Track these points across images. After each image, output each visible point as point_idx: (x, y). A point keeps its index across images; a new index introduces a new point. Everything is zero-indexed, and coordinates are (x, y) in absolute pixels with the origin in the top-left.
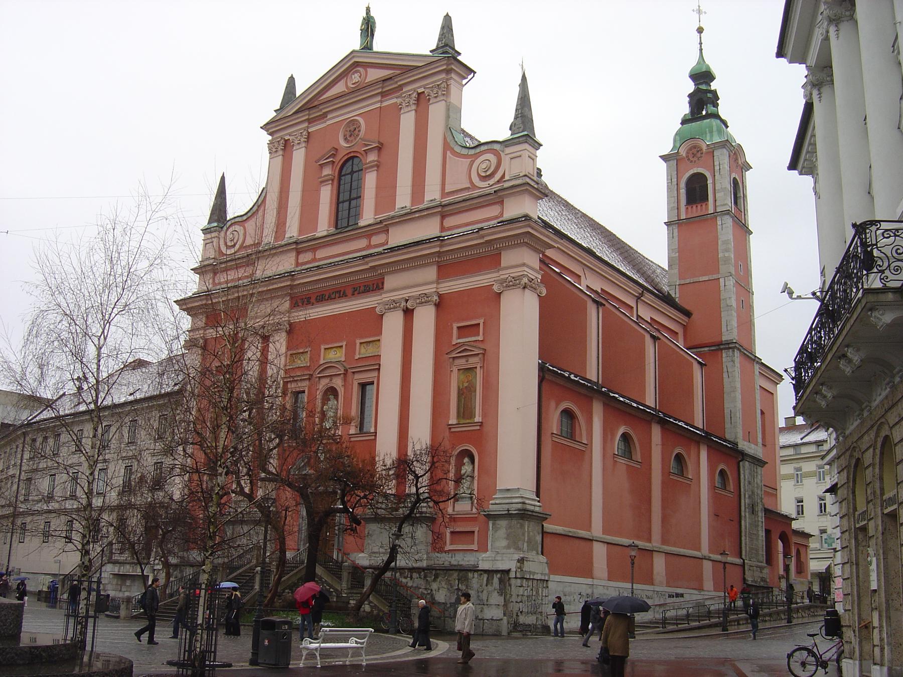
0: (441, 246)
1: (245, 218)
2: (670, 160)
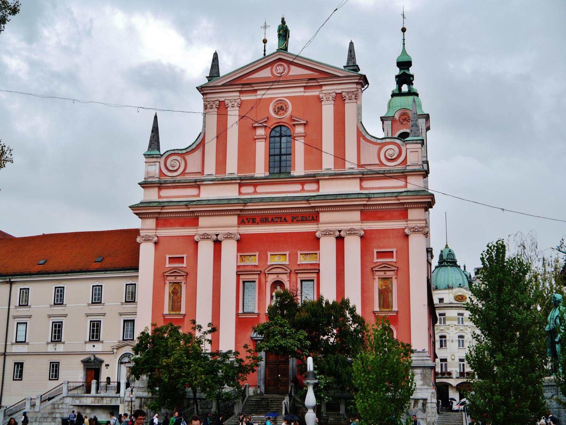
0: (368, 201)
1: (184, 152)
2: (387, 120)
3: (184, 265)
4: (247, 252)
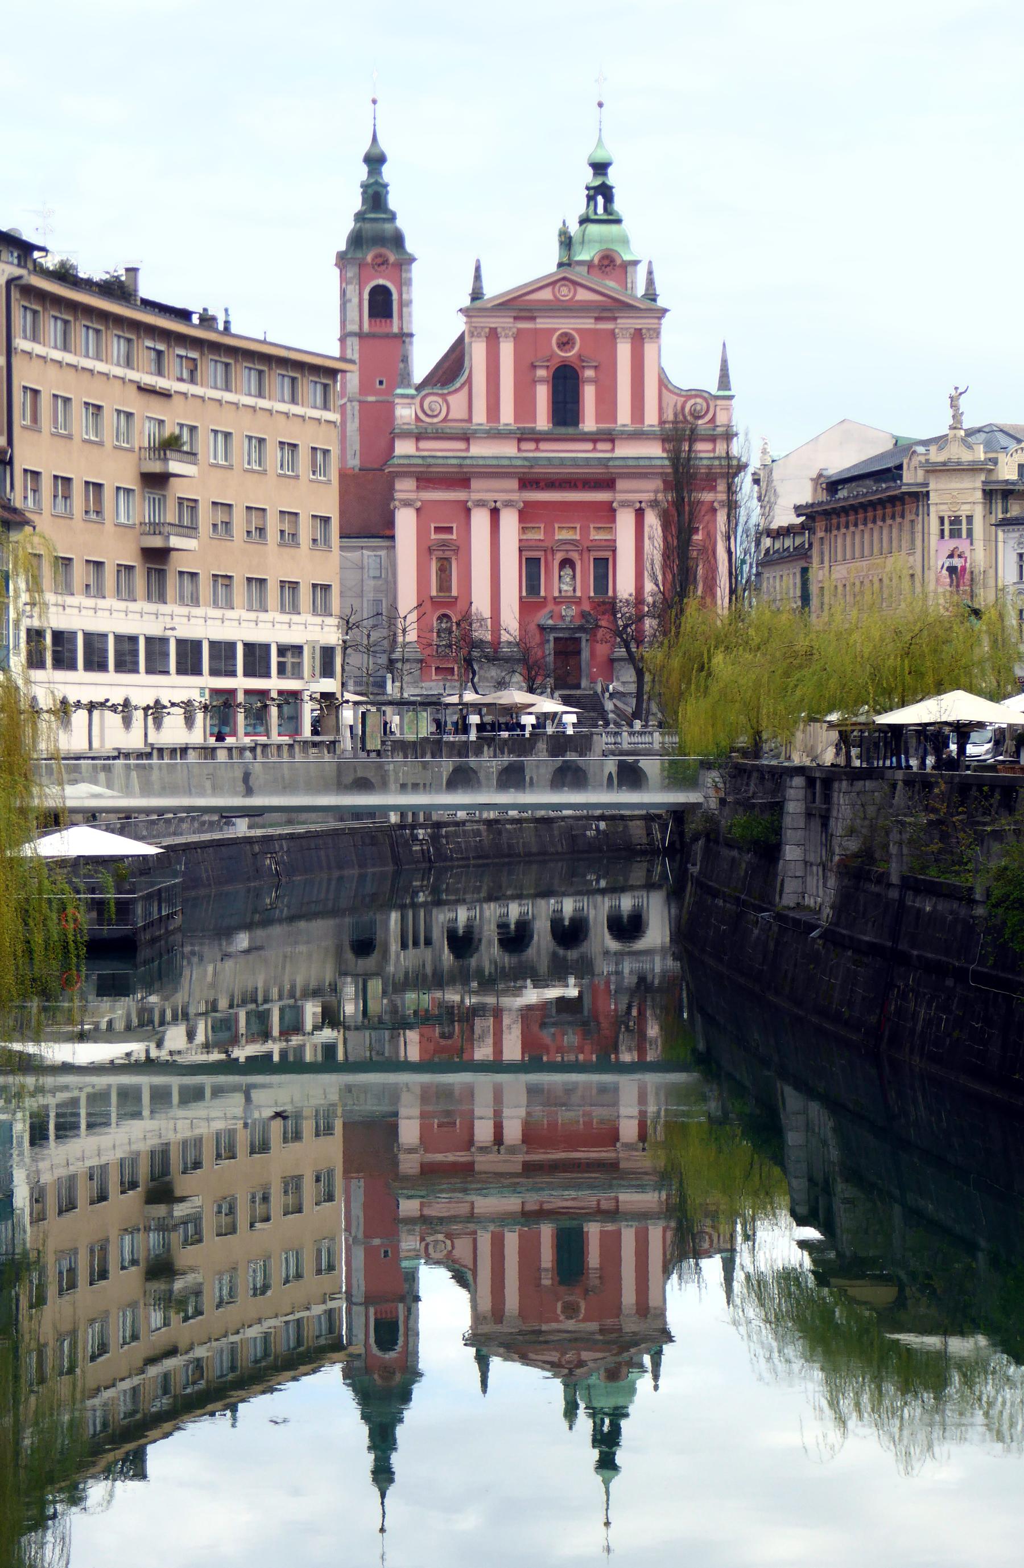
1: (445, 391)
3: (454, 537)
4: (531, 522)
